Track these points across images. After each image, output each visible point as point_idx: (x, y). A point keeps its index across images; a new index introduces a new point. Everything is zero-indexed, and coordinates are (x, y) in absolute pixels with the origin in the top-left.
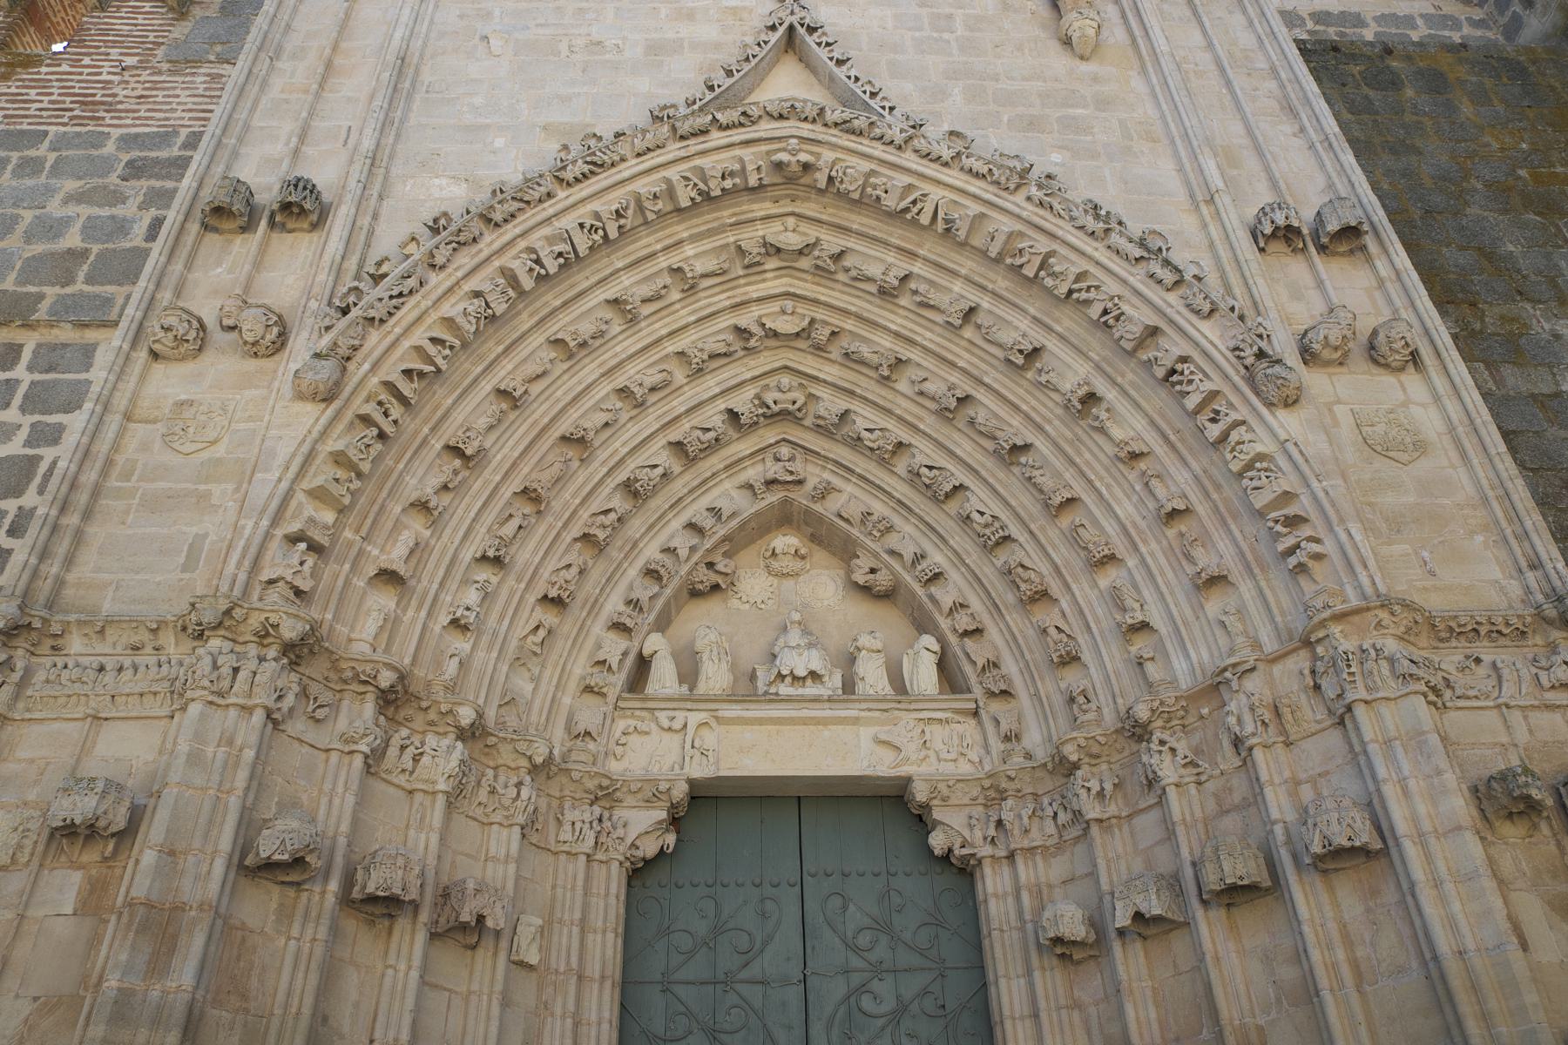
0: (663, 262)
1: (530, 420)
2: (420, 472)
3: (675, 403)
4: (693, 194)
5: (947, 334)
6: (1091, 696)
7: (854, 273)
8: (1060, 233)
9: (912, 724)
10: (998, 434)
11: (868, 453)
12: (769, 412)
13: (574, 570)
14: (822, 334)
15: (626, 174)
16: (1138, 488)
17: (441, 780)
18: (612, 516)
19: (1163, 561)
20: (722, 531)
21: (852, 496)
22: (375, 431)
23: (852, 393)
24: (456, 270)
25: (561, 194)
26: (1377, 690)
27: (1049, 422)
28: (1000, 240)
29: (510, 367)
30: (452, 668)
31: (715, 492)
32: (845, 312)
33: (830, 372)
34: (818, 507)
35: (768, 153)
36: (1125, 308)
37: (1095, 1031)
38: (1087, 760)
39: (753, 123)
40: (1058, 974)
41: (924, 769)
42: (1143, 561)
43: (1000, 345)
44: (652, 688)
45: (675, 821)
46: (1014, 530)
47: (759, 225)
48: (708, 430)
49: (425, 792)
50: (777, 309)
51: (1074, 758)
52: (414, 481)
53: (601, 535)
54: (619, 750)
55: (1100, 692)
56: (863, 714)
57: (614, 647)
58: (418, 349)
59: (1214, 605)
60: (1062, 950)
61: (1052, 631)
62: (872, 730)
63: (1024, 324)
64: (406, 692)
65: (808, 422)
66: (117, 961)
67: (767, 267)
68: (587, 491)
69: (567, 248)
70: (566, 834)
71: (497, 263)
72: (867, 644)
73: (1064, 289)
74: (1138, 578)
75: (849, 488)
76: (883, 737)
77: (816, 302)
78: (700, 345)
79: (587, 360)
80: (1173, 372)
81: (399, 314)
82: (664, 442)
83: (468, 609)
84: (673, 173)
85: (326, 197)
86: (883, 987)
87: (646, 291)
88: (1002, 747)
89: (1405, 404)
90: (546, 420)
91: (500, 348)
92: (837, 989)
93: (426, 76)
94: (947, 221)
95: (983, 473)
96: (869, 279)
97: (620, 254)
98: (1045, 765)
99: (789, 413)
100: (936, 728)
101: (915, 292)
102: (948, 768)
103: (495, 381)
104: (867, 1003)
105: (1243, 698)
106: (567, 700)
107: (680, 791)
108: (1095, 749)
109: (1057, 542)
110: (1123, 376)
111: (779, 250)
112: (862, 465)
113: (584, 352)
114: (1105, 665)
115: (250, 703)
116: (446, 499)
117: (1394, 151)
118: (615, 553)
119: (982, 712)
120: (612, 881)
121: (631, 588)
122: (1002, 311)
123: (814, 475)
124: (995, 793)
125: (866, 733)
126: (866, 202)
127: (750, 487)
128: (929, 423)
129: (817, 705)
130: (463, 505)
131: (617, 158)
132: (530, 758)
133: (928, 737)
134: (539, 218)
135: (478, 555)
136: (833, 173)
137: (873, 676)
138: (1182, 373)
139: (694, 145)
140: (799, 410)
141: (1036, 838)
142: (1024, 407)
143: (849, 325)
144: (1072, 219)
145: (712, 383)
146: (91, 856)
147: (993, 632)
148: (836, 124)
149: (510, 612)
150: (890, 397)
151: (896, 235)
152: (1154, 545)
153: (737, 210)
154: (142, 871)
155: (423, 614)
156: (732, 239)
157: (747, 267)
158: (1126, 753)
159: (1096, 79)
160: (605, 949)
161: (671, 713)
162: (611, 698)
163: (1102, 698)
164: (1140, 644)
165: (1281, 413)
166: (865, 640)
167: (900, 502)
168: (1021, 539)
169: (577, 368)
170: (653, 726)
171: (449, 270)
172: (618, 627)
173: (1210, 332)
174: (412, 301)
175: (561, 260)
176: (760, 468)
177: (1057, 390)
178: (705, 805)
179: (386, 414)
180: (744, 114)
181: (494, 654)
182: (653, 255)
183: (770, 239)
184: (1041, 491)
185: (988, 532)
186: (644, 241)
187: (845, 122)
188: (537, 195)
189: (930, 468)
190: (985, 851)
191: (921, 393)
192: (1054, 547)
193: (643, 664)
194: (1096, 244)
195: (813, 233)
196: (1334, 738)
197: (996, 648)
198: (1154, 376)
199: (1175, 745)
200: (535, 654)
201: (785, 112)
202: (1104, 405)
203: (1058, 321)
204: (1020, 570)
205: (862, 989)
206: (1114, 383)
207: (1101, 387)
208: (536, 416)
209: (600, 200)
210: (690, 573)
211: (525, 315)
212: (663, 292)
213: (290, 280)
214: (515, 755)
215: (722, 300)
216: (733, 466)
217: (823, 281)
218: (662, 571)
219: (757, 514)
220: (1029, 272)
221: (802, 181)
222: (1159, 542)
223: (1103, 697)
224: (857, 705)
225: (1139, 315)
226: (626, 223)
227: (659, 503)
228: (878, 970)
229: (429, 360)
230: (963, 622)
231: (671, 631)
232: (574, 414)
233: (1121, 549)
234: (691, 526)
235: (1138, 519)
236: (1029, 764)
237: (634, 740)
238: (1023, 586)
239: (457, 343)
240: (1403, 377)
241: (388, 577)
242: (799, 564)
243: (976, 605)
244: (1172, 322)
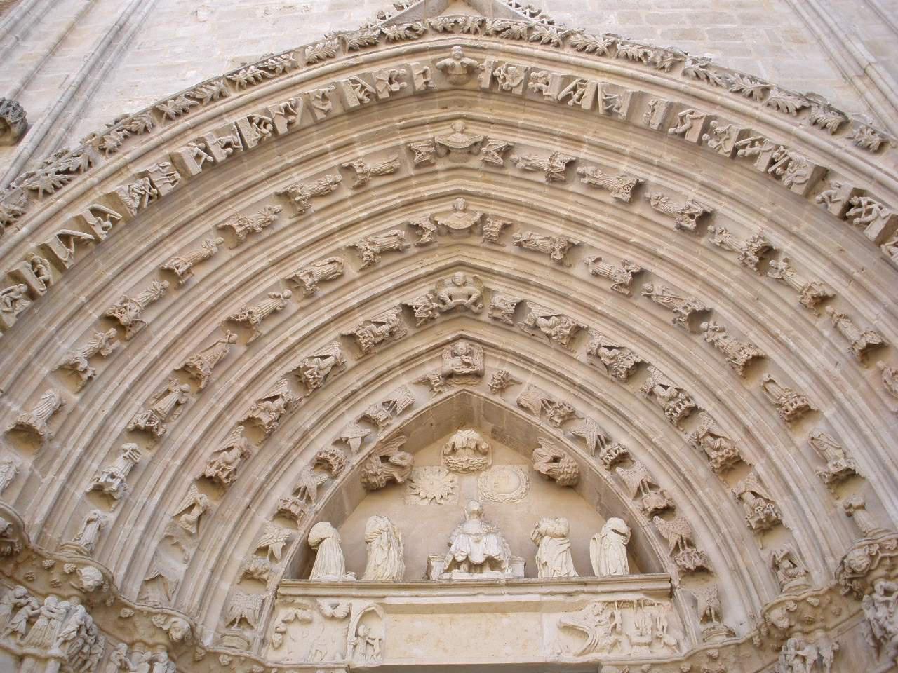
0: (334, 161)
1: (196, 303)
2: (74, 338)
3: (348, 297)
4: (361, 96)
5: (618, 213)
6: (797, 560)
7: (521, 164)
8: (719, 98)
9: (600, 607)
11: (546, 341)
12: (445, 308)
13: (236, 452)
14: (493, 227)
15: (297, 78)
16: (826, 333)
17: (56, 644)
18: (279, 402)
19: (862, 404)
20: (396, 423)
21: (530, 386)
22: (23, 288)
23: (526, 283)
24: (125, 154)
25: (233, 95)
27: (727, 285)
28: (661, 111)
29: (175, 249)
30: (90, 533)
31: (391, 388)
32: (516, 204)
33: (505, 265)
34: (497, 399)
35: (434, 61)
36: (791, 154)
38: (798, 627)
39: (420, 36)
41: (616, 655)
42: (841, 408)
43: (671, 216)
44: (317, 575)
46: (700, 400)
47: (428, 128)
48: (383, 324)
49: (37, 658)
51: (784, 624)
52: (66, 346)
53: (266, 419)
54: (277, 638)
55: (807, 555)
56: (545, 598)
58: (79, 219)
61: (748, 497)
63: (692, 192)
64: (26, 547)
65: (485, 317)
67: (438, 167)
68: (254, 380)
69: (238, 139)
71: (167, 151)
72: (551, 530)
73: (729, 147)
74: (837, 426)
75: (529, 380)
76: (570, 622)
77: (486, 197)
78: (371, 239)
79: (256, 250)
80: (849, 206)
81: (65, 189)
82: (336, 334)
83: (113, 476)
84: (343, 79)
87: (316, 186)
88: (702, 628)
90: (210, 302)
91: (166, 231)
94: (606, 102)
95: (665, 347)
96: (538, 170)
97: (292, 153)
98: (751, 640)
99: (467, 309)
100: (629, 612)
101: (583, 175)
102: (644, 653)
103: (159, 261)
106: (225, 586)
108: (808, 613)
109: (747, 405)
110: (798, 225)
111: (449, 151)
112: (541, 355)
113: (252, 242)
116: (99, 368)
118: (284, 442)
119: (677, 592)
121: (299, 477)
122: (671, 183)
123: (494, 368)
125: (551, 621)
126: (528, 96)
127: (426, 382)
128: (607, 304)
129: (494, 591)
130: (119, 378)
131: (288, 64)
132: (167, 632)
133: (617, 620)
134: (210, 113)
135: (131, 427)
136: (496, 73)
137: (555, 560)
138: (859, 206)
139: (363, 56)
140: (475, 304)
142: (701, 273)
143: (520, 217)
144: (730, 84)
145: (385, 279)
147: (687, 512)
148: (497, 33)
149: (163, 487)
150: (567, 283)
151: (562, 125)
152: (850, 390)
153: (407, 115)
155: (63, 476)
156: (402, 142)
157: (418, 166)
158: (844, 615)
161: (334, 601)
162: (272, 586)
163: (809, 561)
164: (851, 494)
166: (546, 525)
167: (581, 388)
168: (709, 409)
169: (246, 256)
170: (316, 616)
171: (117, 155)
172: (284, 515)
174: (78, 179)
175: (230, 150)
176: (437, 365)
177: (732, 251)
179: (38, 274)
180: (410, 28)
181: (141, 527)
182: (324, 154)
183: (438, 140)
184: (725, 354)
185: (672, 403)
186: (316, 143)
188: (209, 94)
189: (610, 348)
191: (596, 275)
192: (745, 411)
193: (309, 553)
194: (755, 104)
195: (479, 133)
197: (689, 525)
198: (830, 215)
200: (190, 535)
201: (449, 27)
202: (782, 257)
203: (726, 184)
204: (709, 438)
206: (792, 235)
207: (776, 240)
208: (201, 299)
209: (273, 102)
210: (362, 464)
211: (194, 203)
212: (333, 187)
214: (152, 631)
215: (395, 199)
217: (493, 178)
218: (332, 460)
219: (435, 407)
220: (692, 137)
221: (468, 86)
222: (856, 386)
223: (811, 560)
224: (539, 590)
225: (805, 161)
226: (297, 119)
227: (331, 396)
229: (88, 228)
230: (653, 500)
231: (347, 525)
233: (815, 401)
234: (366, 420)
235: (831, 367)
236: (733, 640)
237: (294, 630)
238: (713, 454)
239: (118, 216)
242: (479, 460)
243: (665, 483)
244: (842, 162)
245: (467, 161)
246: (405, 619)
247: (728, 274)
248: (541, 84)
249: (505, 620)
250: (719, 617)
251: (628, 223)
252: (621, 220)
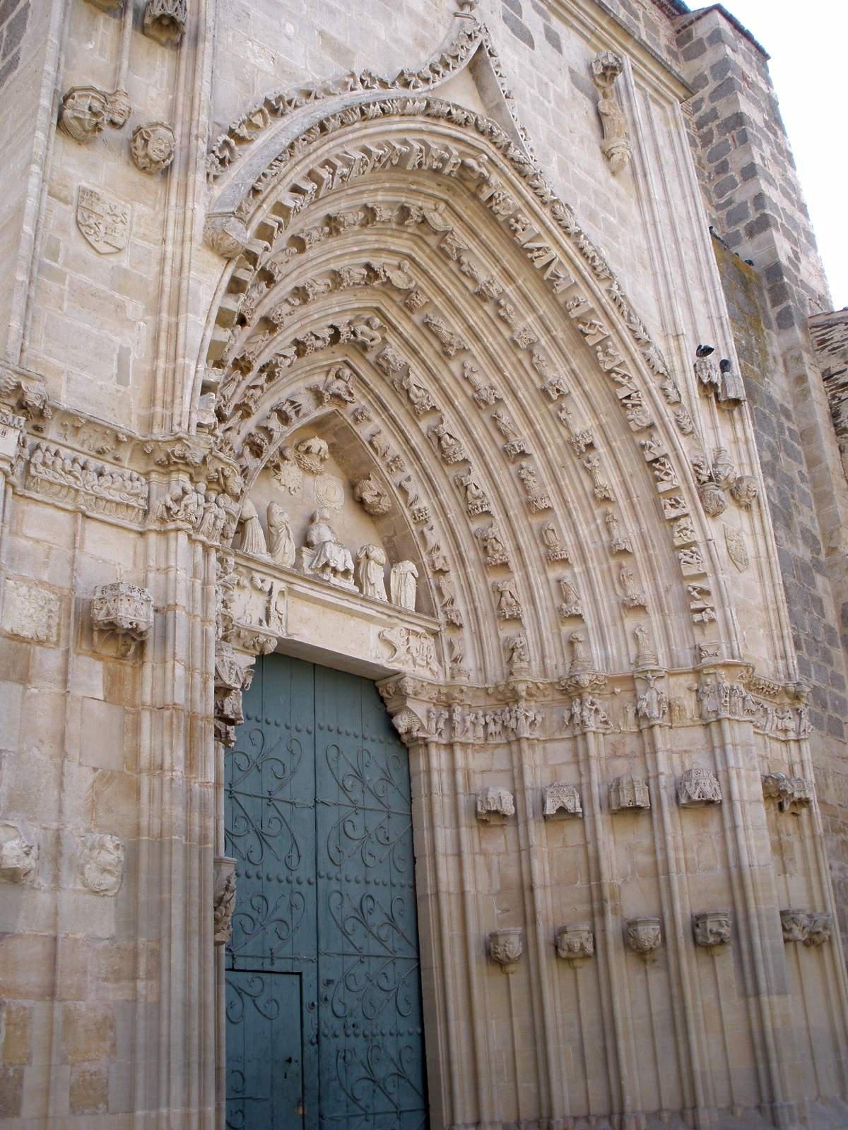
10: (512, 438)
16: (599, 521)
23: (415, 352)
26: (735, 714)
32: (441, 291)
33: (406, 328)
37: (495, 872)
40: (475, 830)
50: (396, 263)
59: (630, 622)
60: (488, 819)
62: (378, 629)
63: (563, 370)
73: (608, 367)
96: (474, 280)
105: (655, 695)
108: (534, 691)
115: (210, 543)
125: (375, 629)
141: (470, 738)
144: (630, 321)
148: (512, 159)
151: (508, 260)
161: (264, 577)
173: (683, 443)
177: (567, 428)
184: (527, 492)
187: (519, 162)
196: (699, 733)
199: (599, 707)
207: (598, 442)
213: (153, 93)
217: (436, 259)
225: (647, 414)
244: (664, 425)
245: (427, 234)
246: (299, 602)
247: (553, 438)
248: (519, 226)
249: (354, 622)
251: (508, 357)
252: (504, 352)
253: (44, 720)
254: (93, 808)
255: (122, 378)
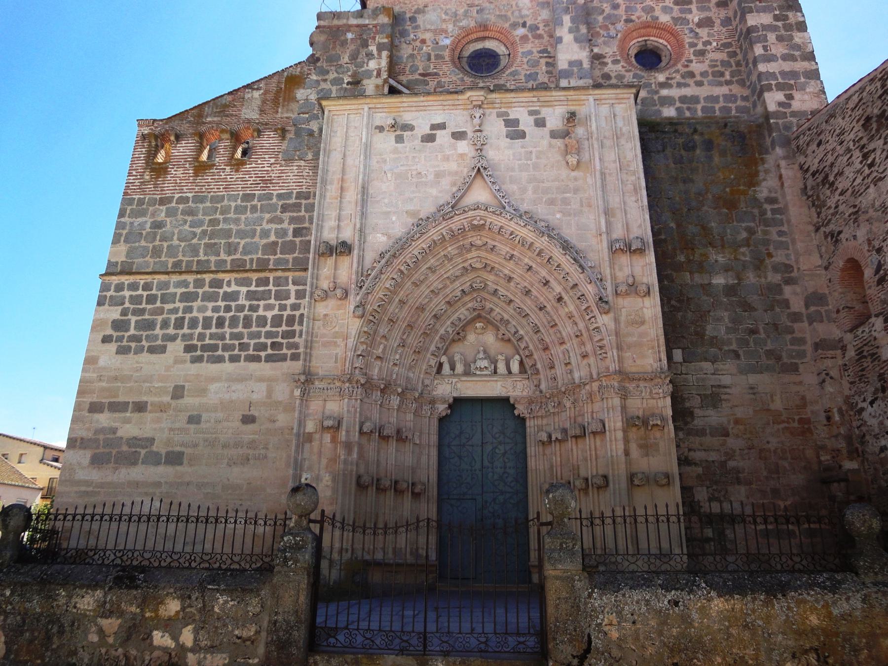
34: (488, 316)
41: (514, 394)
44: (443, 372)
45: (450, 407)
57: (433, 362)
59: (585, 362)
66: (342, 452)
70: (424, 412)
85: (349, 242)
86: (502, 448)
89: (642, 308)
92: (489, 448)
93: (371, 191)
104: (497, 451)
107: (451, 400)
114: (559, 370)
117: (684, 182)
120: (435, 423)
124: (531, 402)
125: (499, 383)
141: (540, 414)
143: (496, 266)
146: (331, 431)
147: (535, 356)
154: (342, 435)
159: (576, 179)
160: (434, 438)
165: (604, 316)
178: (458, 403)
190: (528, 416)
193: (441, 365)
205: (496, 447)
207: (564, 295)
213: (344, 273)
216: (464, 305)
228: (500, 443)
230: (527, 353)
232: (420, 300)
237: (439, 386)
240: (645, 299)
241: (378, 358)
243: (531, 347)
250: (539, 386)
253: (316, 450)
254: (327, 467)
255: (336, 362)
